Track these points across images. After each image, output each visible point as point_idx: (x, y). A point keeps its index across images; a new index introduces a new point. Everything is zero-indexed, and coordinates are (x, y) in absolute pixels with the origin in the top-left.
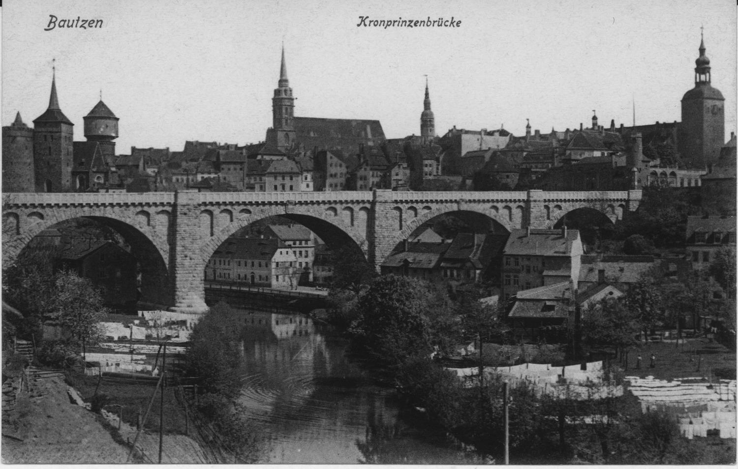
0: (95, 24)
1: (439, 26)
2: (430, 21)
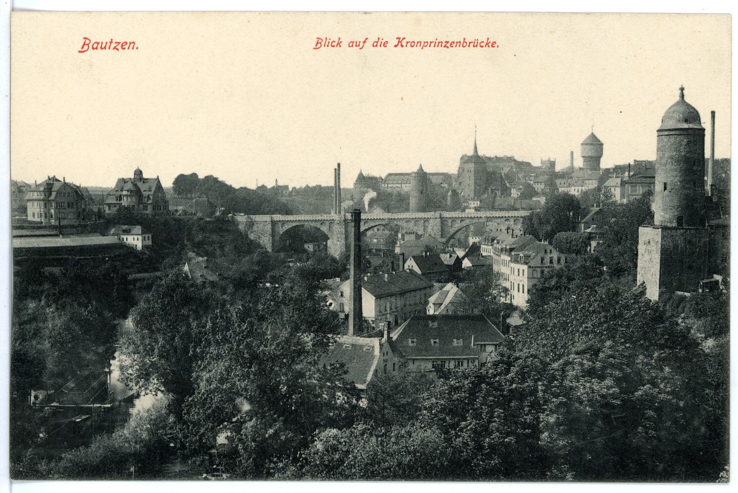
1: (474, 46)
2: (466, 43)
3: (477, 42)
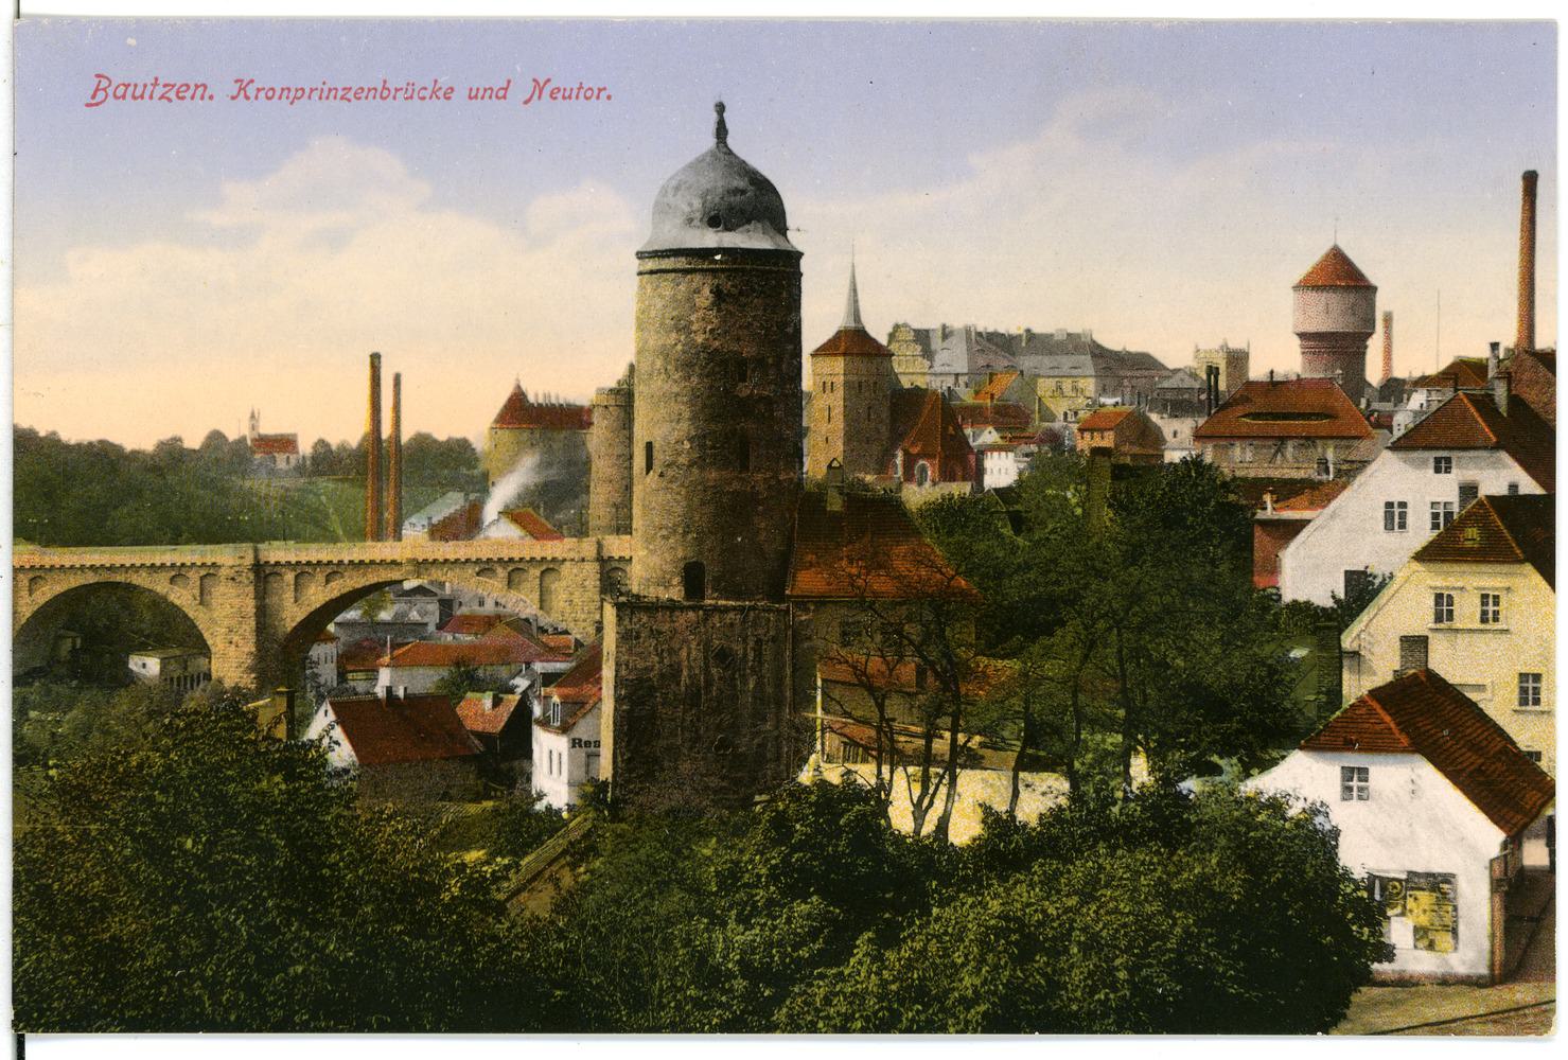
0: (364, 95)
2: (389, 91)
3: (413, 90)
